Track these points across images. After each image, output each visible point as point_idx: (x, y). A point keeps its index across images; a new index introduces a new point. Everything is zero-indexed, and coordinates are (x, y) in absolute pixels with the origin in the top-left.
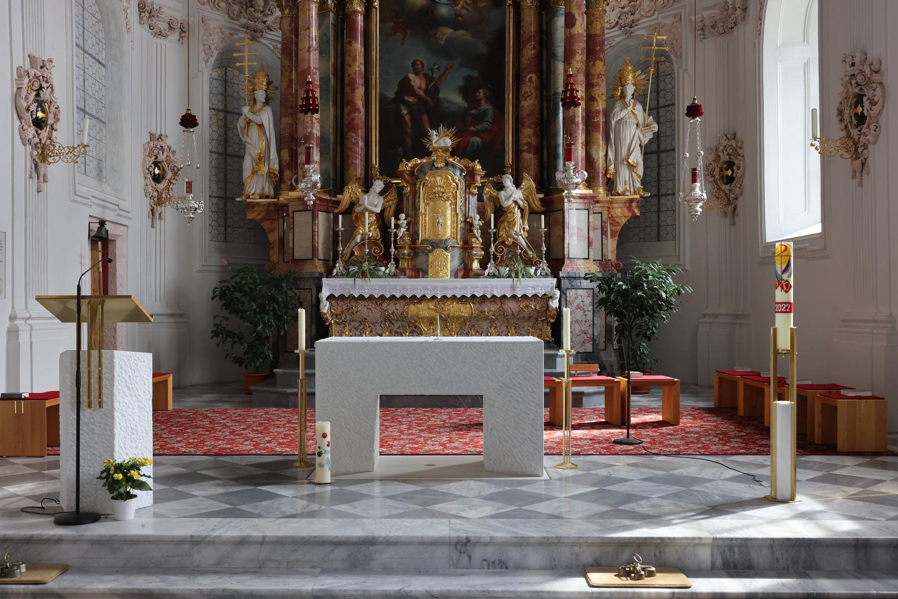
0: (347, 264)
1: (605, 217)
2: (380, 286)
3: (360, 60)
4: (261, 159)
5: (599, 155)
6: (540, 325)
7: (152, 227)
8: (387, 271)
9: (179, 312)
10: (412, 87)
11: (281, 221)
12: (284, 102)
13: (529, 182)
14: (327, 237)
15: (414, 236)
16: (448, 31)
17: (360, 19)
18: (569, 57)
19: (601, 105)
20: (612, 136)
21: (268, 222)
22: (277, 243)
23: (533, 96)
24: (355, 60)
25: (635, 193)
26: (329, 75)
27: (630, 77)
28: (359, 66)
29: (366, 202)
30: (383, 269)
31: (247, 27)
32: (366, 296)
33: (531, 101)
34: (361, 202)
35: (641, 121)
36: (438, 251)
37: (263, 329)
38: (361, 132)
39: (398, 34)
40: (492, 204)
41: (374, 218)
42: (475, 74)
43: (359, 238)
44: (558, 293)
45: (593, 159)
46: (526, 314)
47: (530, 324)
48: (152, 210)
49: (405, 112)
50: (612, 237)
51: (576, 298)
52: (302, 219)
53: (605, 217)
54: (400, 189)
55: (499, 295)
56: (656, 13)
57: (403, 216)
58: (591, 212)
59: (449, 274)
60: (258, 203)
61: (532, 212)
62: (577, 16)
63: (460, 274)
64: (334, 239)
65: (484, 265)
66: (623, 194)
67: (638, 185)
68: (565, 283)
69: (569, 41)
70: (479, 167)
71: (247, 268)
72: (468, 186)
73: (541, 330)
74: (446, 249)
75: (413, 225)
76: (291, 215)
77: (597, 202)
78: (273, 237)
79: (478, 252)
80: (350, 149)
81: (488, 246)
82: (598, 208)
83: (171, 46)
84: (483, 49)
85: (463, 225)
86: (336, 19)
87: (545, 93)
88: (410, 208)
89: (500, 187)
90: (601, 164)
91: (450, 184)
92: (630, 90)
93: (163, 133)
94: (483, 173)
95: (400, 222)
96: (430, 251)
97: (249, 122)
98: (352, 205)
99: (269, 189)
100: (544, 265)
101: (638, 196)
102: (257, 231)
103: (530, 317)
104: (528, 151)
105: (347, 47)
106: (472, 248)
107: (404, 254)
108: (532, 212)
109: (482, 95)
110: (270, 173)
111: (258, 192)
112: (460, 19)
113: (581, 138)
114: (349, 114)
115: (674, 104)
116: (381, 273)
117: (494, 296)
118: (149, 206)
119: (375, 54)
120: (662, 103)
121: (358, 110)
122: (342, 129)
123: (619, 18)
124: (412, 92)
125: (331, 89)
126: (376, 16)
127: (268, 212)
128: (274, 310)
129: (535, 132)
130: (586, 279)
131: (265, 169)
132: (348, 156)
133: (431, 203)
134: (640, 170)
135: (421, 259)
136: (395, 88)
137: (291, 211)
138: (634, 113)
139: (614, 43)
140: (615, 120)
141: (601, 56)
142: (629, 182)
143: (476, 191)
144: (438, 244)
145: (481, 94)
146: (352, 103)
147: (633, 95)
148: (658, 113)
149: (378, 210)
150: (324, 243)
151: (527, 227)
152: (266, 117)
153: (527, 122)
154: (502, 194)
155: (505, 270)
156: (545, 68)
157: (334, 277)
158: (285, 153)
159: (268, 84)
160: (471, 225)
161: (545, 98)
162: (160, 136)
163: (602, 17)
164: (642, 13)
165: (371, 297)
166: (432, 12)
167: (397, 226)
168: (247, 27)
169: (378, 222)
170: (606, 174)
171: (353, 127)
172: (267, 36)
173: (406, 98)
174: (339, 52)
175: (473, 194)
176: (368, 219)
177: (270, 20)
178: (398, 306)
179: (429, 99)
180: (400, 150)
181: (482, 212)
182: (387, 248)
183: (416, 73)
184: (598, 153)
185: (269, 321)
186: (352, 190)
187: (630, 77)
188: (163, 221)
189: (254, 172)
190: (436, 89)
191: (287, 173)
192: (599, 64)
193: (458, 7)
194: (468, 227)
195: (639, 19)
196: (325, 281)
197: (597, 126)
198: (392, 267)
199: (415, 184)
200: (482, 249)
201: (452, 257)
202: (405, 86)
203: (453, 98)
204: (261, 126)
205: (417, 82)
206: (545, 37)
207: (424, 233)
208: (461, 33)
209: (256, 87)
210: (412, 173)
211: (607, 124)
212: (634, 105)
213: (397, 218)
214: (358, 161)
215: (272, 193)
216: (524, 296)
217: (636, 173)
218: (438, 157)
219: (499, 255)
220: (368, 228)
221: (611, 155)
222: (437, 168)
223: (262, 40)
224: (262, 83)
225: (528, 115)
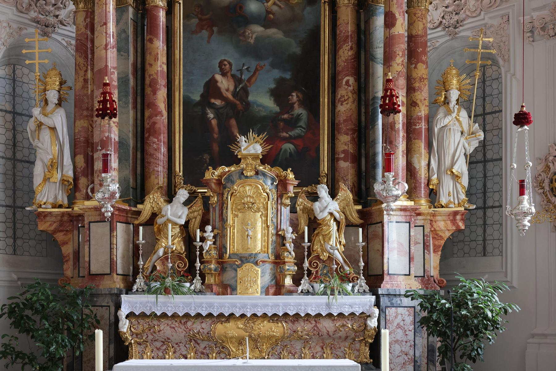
11: (76, 232)
18: (388, 59)
21: (62, 234)
37: (56, 349)
71: (38, 283)
102: (50, 243)
115: (501, 111)
128: (69, 329)
148: (484, 120)
163: (424, 17)
185: (63, 341)
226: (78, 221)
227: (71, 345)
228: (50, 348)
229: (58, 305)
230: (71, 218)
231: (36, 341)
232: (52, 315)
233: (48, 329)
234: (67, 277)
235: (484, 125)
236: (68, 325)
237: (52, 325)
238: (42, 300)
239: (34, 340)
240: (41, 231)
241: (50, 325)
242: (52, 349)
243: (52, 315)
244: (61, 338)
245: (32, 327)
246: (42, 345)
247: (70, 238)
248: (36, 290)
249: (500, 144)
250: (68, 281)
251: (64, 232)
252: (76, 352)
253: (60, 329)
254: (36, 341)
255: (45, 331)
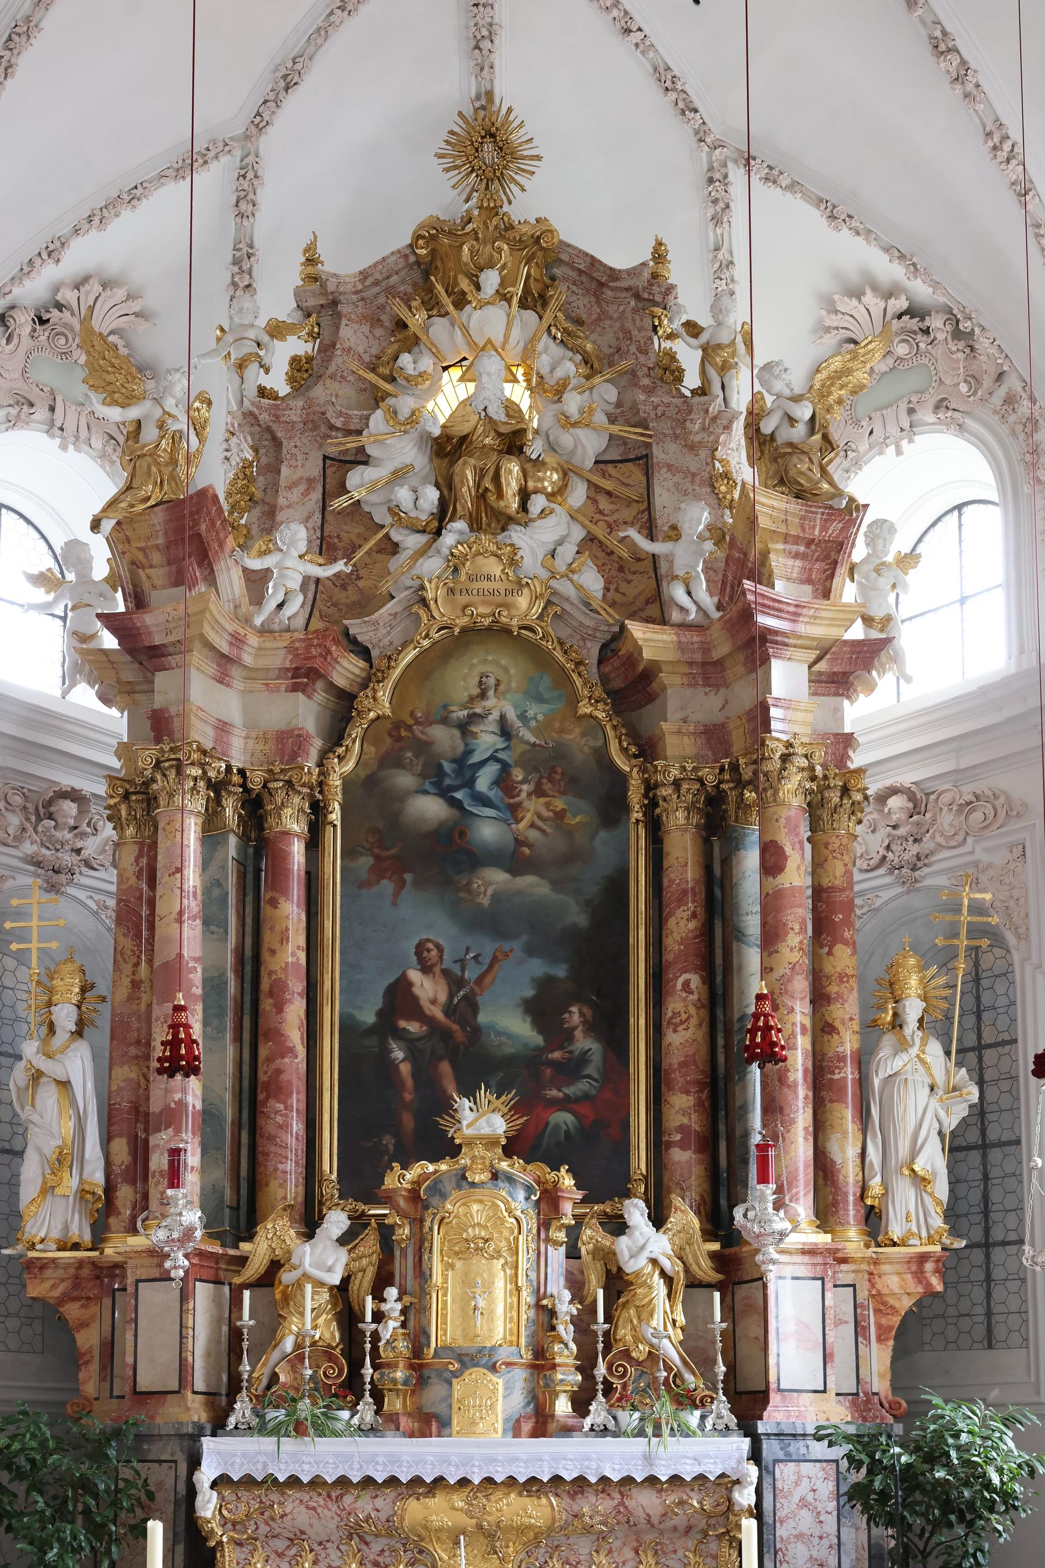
0: (260, 1402)
1: (863, 1294)
2: (337, 1455)
3: (297, 939)
4: (64, 1159)
5: (845, 1152)
6: (713, 1546)
8: (356, 1420)
10: (415, 999)
11: (107, 1302)
12: (118, 1031)
13: (685, 1216)
14: (214, 1340)
15: (418, 1340)
16: (497, 877)
17: (297, 851)
19: (847, 1042)
20: (875, 1112)
21: (76, 1305)
22: (96, 1353)
23: (694, 1021)
24: (284, 939)
25: (931, 1240)
26: (223, 974)
27: (914, 981)
28: (292, 953)
29: (307, 1261)
30: (345, 1414)
31: (37, 863)
32: (305, 1479)
33: (689, 1034)
34: (294, 1260)
35: (940, 1078)
36: (475, 1374)
37: (60, 1556)
38: (297, 1100)
39: (385, 882)
40: (599, 1265)
41: (326, 1296)
42: (561, 971)
43: (288, 1344)
44: (753, 1471)
45: (833, 1162)
46: (680, 1520)
47: (691, 1543)
49: (399, 1054)
50: (879, 1340)
51: (797, 1484)
52: (155, 1300)
53: (863, 1294)
54: (386, 1233)
55: (615, 1477)
56: (970, 840)
57: (392, 1293)
58: (829, 1285)
59: (500, 1426)
60: (54, 1260)
61: (693, 1284)
62: (788, 850)
63: (527, 1427)
64: (233, 1344)
65: (581, 1404)
66: (904, 1243)
67: (938, 1222)
68: (770, 1449)
69: (772, 904)
70: (568, 1181)
71: (25, 1413)
72: (544, 1225)
73: (715, 1557)
74: (493, 1368)
75: (415, 1316)
76: (130, 1289)
77: (844, 1260)
78: (89, 1339)
79: (568, 1377)
80: (271, 1138)
81: (590, 1363)
82: (846, 1274)
84: (577, 917)
85: (532, 1313)
86: (242, 849)
87: (720, 1015)
88: (410, 1275)
89: (618, 1226)
90: (849, 1174)
91: (503, 1221)
92: (913, 1009)
94: (579, 1195)
95: (384, 1307)
96: (456, 1374)
97: (37, 1076)
98: (275, 1266)
99: (80, 1230)
100: (722, 1406)
101: (938, 1248)
102: (51, 1325)
103: (689, 1529)
104: (683, 1146)
105: (266, 910)
106: (554, 1367)
107: (394, 1381)
108: (693, 1284)
109: (576, 1018)
110: (83, 1193)
111: (56, 1234)
112: (526, 850)
113: (802, 1117)
114: (269, 1060)
115: (1015, 1041)
116: (340, 1426)
117: (604, 1480)
119: (331, 926)
120: (988, 1037)
121: (291, 1050)
122: (253, 1094)
123: (888, 848)
124: (415, 1011)
125: (230, 1004)
126: (333, 841)
127: (77, 1281)
128: (87, 1512)
129: (699, 1103)
130: (819, 1439)
131: (71, 1183)
132: (266, 1154)
133: (459, 1264)
134: (942, 1189)
135: (434, 1392)
136: (376, 1002)
137: (130, 1280)
138: (922, 1061)
139: (878, 902)
140: (882, 1075)
141: (847, 935)
142: (917, 1215)
143: (562, 1236)
144: (473, 1358)
145: (575, 1015)
146: (277, 1035)
147: (921, 1021)
148: (980, 1059)
149: (336, 1279)
150: (208, 1355)
151: (681, 1319)
152: (78, 1065)
153: (679, 1078)
154: (623, 1244)
155: (630, 1419)
156: (719, 960)
157: (230, 1434)
158: (121, 1148)
159: (84, 990)
160: (552, 1313)
161: (720, 1027)
163: (845, 849)
164: (940, 840)
165: (317, 1482)
166: (462, 834)
167: (379, 1317)
168: (37, 863)
169: (335, 1305)
170: (862, 1197)
171: (278, 1090)
172: (84, 881)
173: (402, 1024)
174: (249, 920)
175: (557, 1244)
176: (311, 1299)
177: (91, 846)
178: (379, 1503)
179: (456, 1027)
180: (388, 1141)
181: (576, 1285)
182: (355, 1366)
183: (426, 969)
184: (843, 1151)
185: (75, 1538)
186: (275, 1234)
187: (914, 981)
189: (47, 1190)
190: (472, 1005)
191: (125, 1194)
192: (842, 952)
193: (522, 825)
194: (544, 1318)
195: (933, 853)
196: (208, 1443)
197: (839, 1088)
198: (366, 1410)
199: (422, 1221)
200: (578, 1369)
201: (508, 1388)
202: (399, 998)
203: (509, 1024)
204: (65, 1085)
205: (428, 989)
206: (718, 892)
207: (445, 1329)
208: (527, 881)
209: (55, 998)
210: (414, 1195)
211: (863, 1083)
212: (924, 1043)
213: (379, 1297)
214: (290, 1166)
215: (87, 1237)
216: (676, 1480)
217: (931, 1195)
218: (473, 1159)
219: (617, 1383)
220: (312, 1321)
221: (874, 1155)
222: (473, 1185)
223: (70, 890)
224: (69, 987)
225: (682, 1065)
226: (113, 1277)
227: (92, 1548)
228: (45, 1554)
229: (66, 1461)
230: (97, 1272)
231: (15, 1538)
232: (52, 1481)
233: (43, 1512)
234: (86, 1398)
235: (981, 1069)
236: (84, 1503)
237: (52, 1503)
238: (33, 1449)
239: (11, 1536)
240: (34, 1299)
241: (47, 1504)
242: (51, 1555)
243: (52, 1481)
244: (71, 1531)
245: (8, 1508)
246: (29, 1547)
247: (95, 1315)
248: (18, 1428)
249: (1014, 1109)
250: (87, 1407)
251: (83, 1302)
252: (101, 1561)
253: (69, 1512)
254: (15, 1538)
255: (37, 1517)
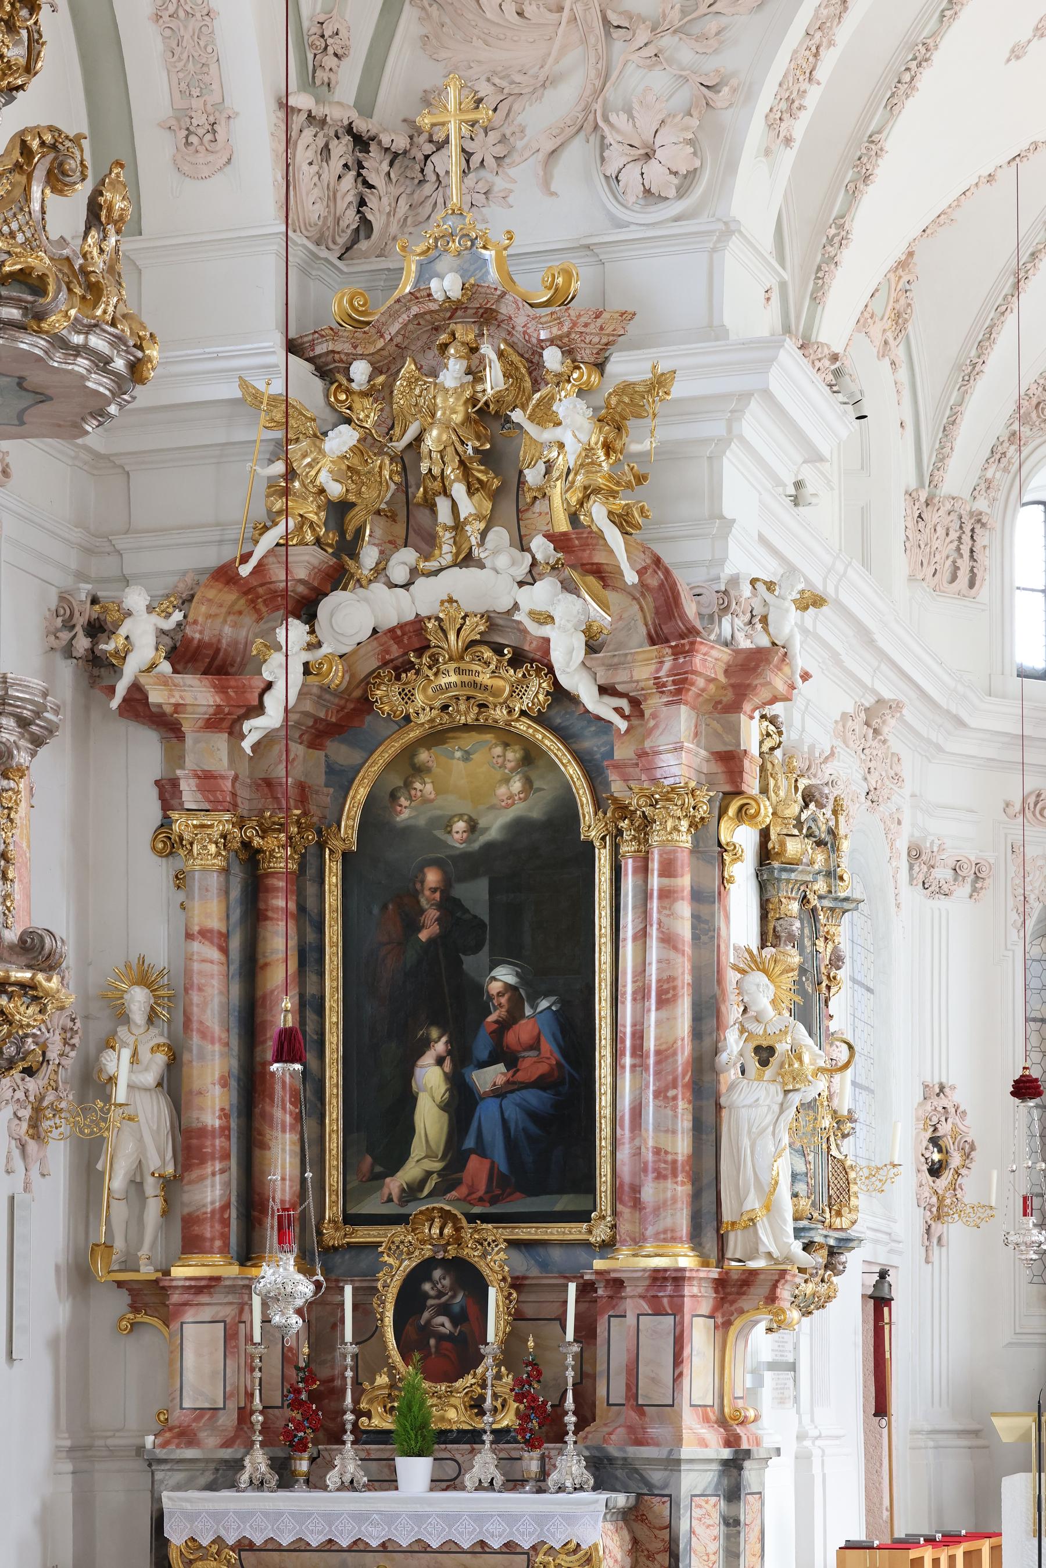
7: (927, 1262)
9: (975, 1426)
48: (928, 1231)
83: (958, 906)
93: (944, 1080)
118: (922, 1222)
162: (942, 1088)
188: (944, 1249)
